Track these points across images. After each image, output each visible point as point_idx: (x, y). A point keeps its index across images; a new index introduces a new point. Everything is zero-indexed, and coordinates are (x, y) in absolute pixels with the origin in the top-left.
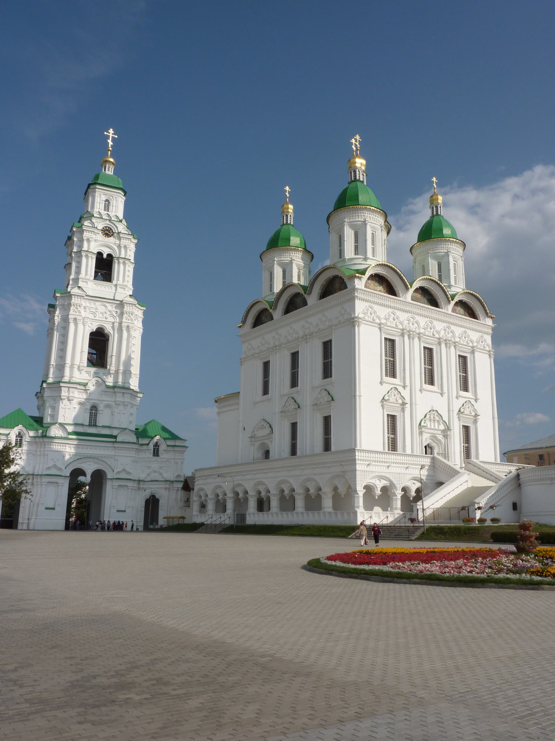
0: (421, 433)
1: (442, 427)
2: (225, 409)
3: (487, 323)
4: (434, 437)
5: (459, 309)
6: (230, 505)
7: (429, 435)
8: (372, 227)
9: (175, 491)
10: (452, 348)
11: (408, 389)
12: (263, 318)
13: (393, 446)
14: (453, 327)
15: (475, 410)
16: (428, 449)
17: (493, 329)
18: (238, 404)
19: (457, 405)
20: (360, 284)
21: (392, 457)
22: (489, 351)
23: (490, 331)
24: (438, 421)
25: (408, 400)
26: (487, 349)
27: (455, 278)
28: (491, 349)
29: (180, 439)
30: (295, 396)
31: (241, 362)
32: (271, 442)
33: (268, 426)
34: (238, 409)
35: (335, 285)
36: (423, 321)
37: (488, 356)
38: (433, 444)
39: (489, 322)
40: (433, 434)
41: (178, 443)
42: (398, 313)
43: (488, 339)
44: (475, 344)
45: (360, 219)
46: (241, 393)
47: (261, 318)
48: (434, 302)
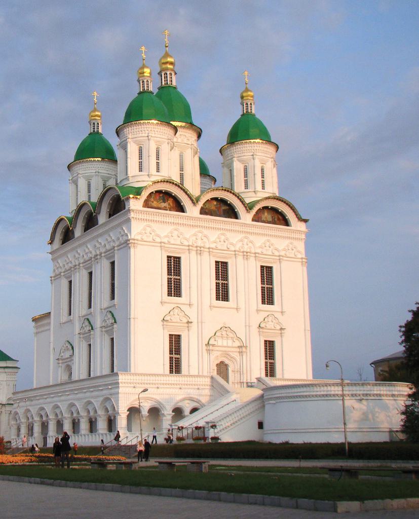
0: (208, 351)
1: (237, 344)
2: (43, 329)
3: (299, 229)
4: (226, 354)
5: (266, 215)
6: (37, 429)
7: (219, 353)
8: (156, 142)
9: (7, 415)
10: (252, 259)
11: (195, 308)
12: (207, 181)
13: (175, 367)
14: (252, 238)
15: (279, 323)
16: (222, 369)
17: (308, 235)
18: (49, 324)
19: (257, 319)
21: (174, 378)
22: (302, 258)
23: (303, 236)
24: (232, 338)
25: (193, 318)
26: (299, 256)
27: (263, 182)
28: (304, 256)
29: (12, 360)
30: (88, 317)
31: (51, 280)
32: (73, 363)
33: (70, 348)
34: (49, 329)
35: (118, 206)
36: (213, 236)
37: (300, 263)
38: (227, 362)
39: (302, 226)
40: (225, 351)
41: (9, 364)
42: (182, 229)
43: (301, 246)
44: (283, 253)
45: (143, 135)
46: (52, 314)
47: (67, 236)
48: (231, 213)
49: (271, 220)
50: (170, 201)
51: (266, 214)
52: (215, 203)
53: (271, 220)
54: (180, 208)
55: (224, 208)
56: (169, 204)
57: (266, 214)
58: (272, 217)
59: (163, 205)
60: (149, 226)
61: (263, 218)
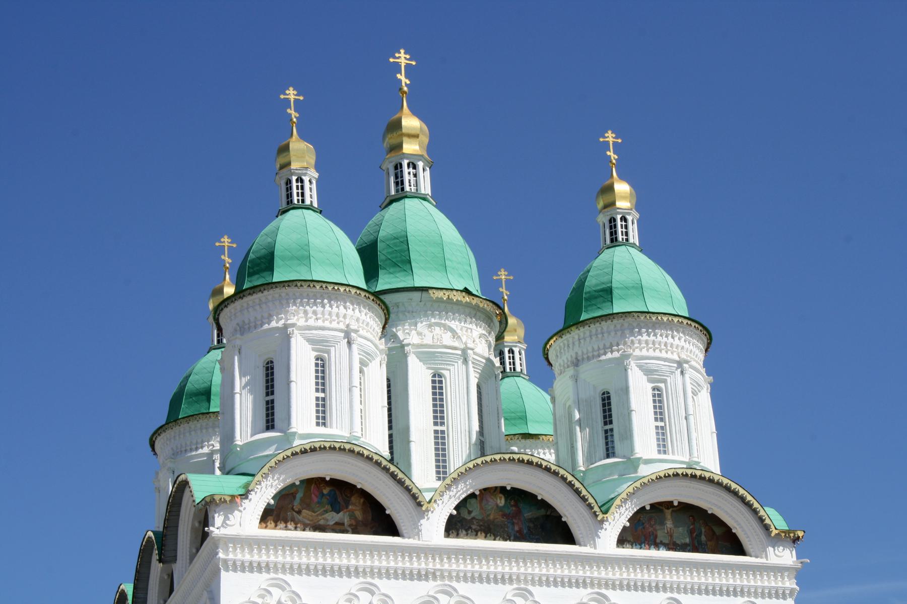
8: (310, 341)
17: (801, 575)
20: (242, 523)
48: (551, 527)
49: (687, 540)
50: (356, 508)
51: (669, 524)
52: (501, 501)
53: (687, 540)
54: (382, 522)
55: (528, 513)
56: (353, 516)
57: (669, 524)
58: (691, 532)
59: (333, 517)
60: (282, 586)
61: (661, 536)
